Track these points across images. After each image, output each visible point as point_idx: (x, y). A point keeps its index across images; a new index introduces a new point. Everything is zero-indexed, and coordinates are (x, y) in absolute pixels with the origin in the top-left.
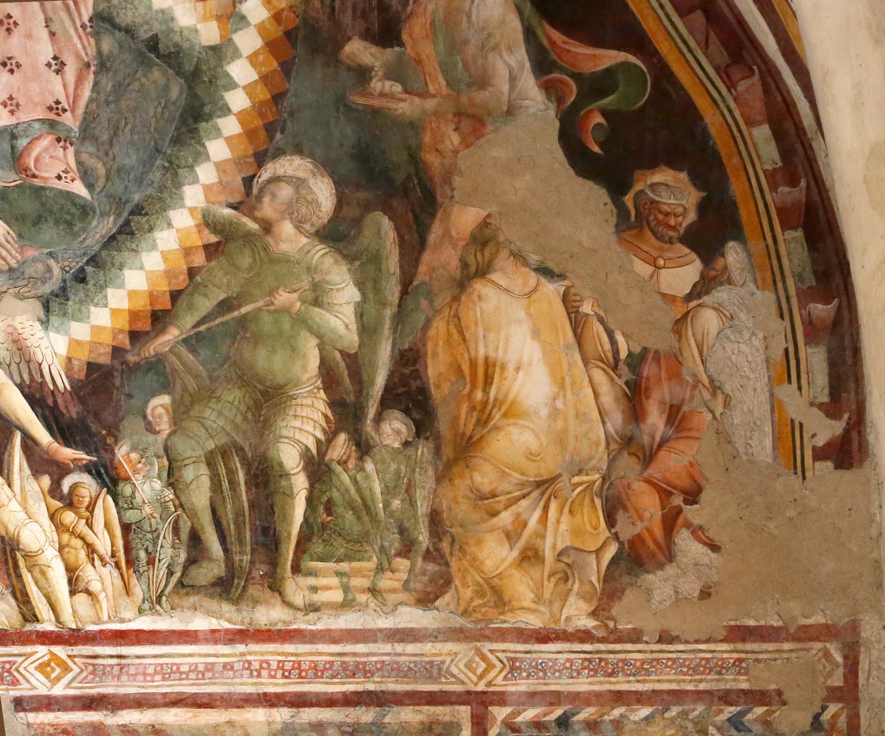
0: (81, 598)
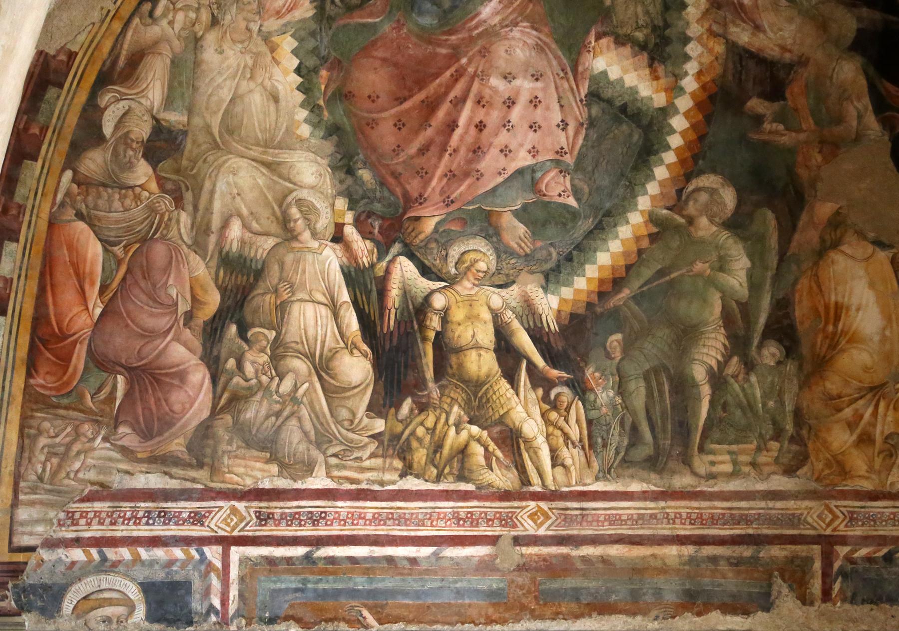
0: (559, 469)
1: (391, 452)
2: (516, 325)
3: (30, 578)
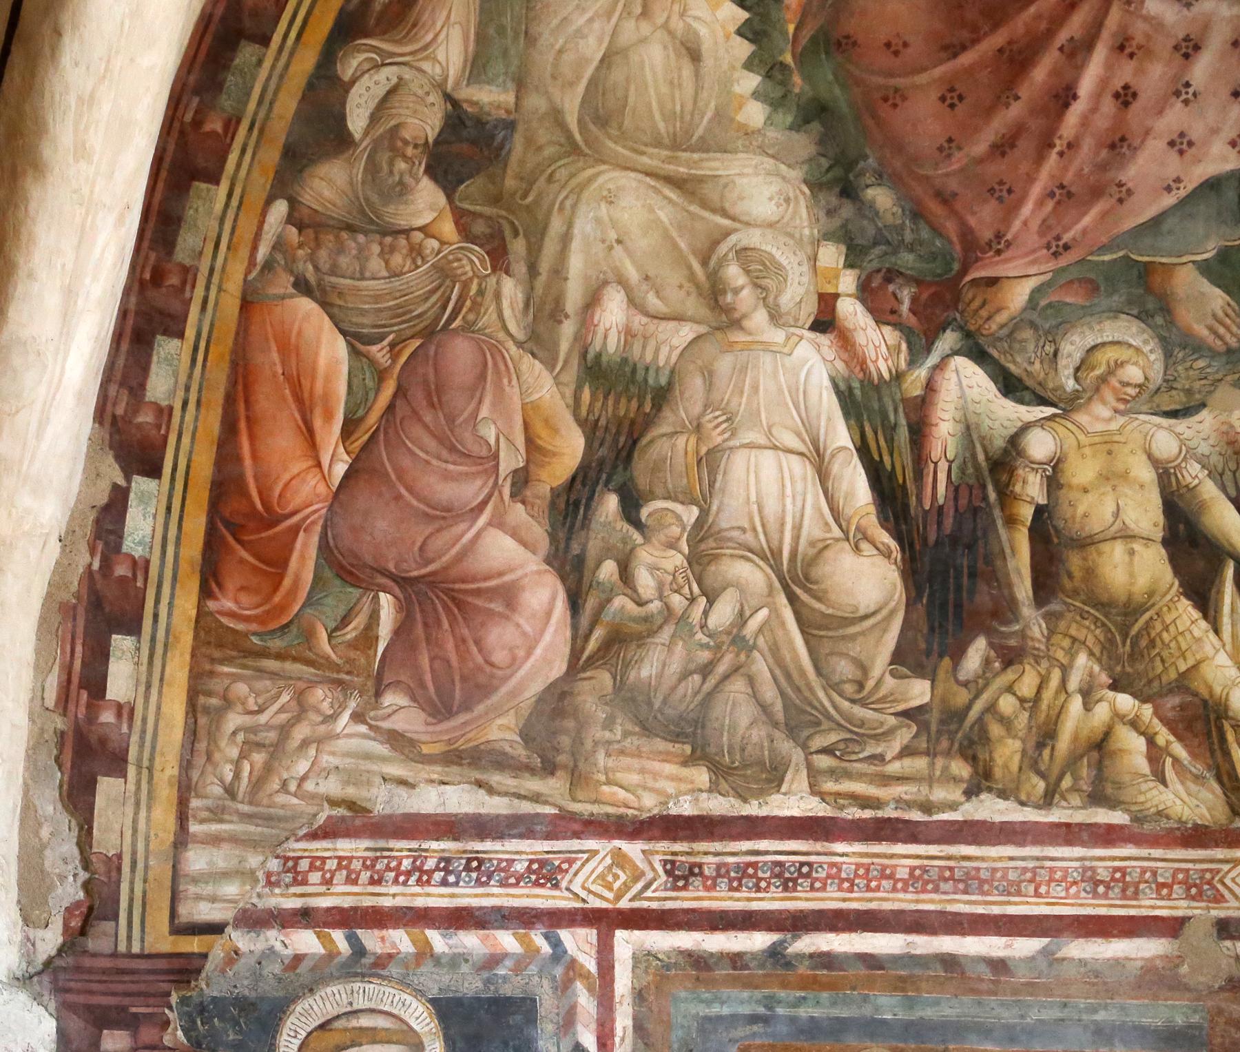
1: (945, 744)
3: (212, 985)
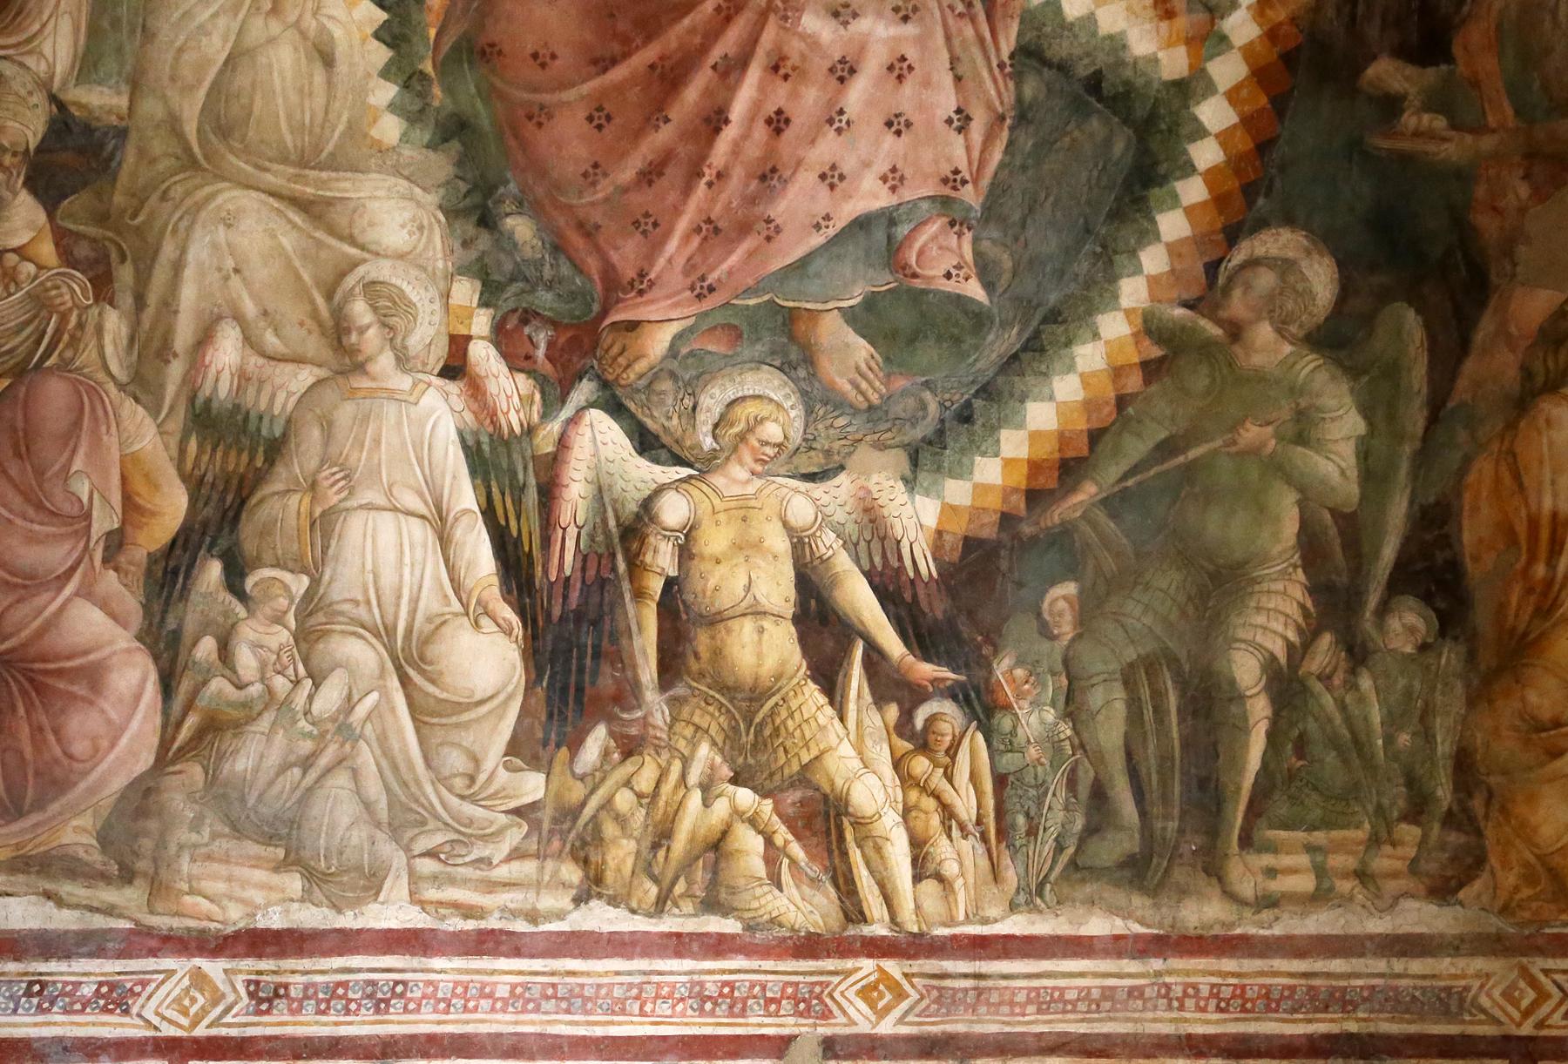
1: (556, 844)
2: (843, 563)
